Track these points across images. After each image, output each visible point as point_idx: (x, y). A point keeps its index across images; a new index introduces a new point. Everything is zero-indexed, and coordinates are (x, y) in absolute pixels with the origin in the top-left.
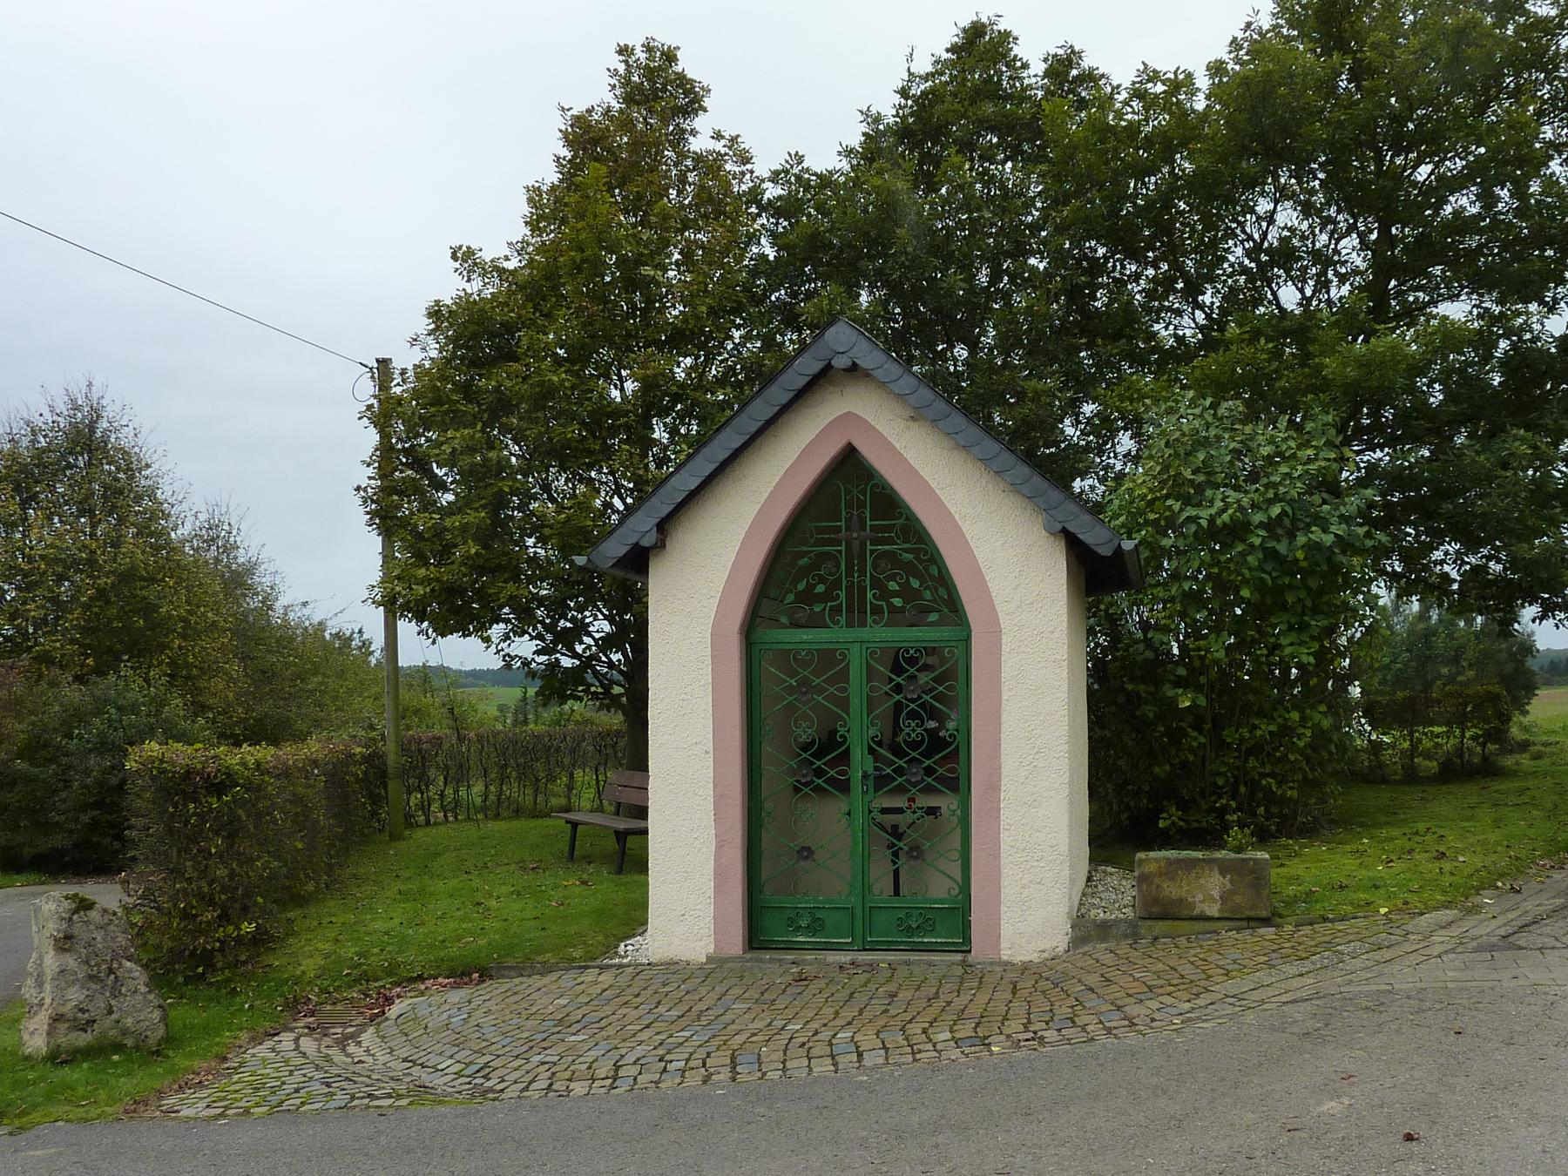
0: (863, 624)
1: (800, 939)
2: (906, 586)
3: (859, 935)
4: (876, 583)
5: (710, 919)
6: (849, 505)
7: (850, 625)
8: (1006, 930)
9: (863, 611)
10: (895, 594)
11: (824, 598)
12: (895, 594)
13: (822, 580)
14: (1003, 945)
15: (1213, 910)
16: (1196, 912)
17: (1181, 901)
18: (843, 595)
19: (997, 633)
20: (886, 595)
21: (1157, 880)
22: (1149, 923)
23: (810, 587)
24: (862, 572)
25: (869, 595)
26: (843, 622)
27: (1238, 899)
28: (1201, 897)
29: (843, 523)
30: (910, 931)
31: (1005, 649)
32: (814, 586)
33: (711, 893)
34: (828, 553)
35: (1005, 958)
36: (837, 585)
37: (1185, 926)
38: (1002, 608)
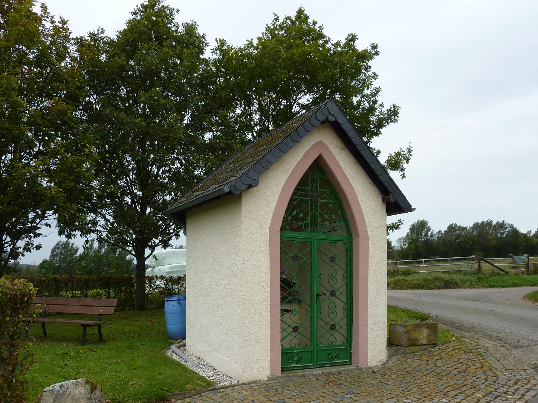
0: (316, 232)
1: (294, 365)
2: (330, 217)
3: (315, 361)
4: (321, 216)
5: (269, 360)
6: (312, 181)
7: (312, 231)
8: (370, 355)
9: (316, 225)
10: (327, 220)
11: (303, 219)
12: (327, 220)
13: (302, 212)
14: (369, 360)
15: (425, 342)
16: (421, 343)
17: (417, 339)
18: (309, 219)
19: (367, 239)
20: (324, 220)
21: (411, 332)
22: (408, 348)
23: (298, 214)
24: (316, 210)
25: (318, 219)
26: (309, 230)
27: (431, 337)
28: (422, 337)
29: (309, 188)
30: (332, 358)
31: (370, 245)
32: (299, 214)
33: (269, 348)
34: (304, 200)
35: (369, 365)
36: (307, 214)
37: (417, 348)
38: (369, 229)
